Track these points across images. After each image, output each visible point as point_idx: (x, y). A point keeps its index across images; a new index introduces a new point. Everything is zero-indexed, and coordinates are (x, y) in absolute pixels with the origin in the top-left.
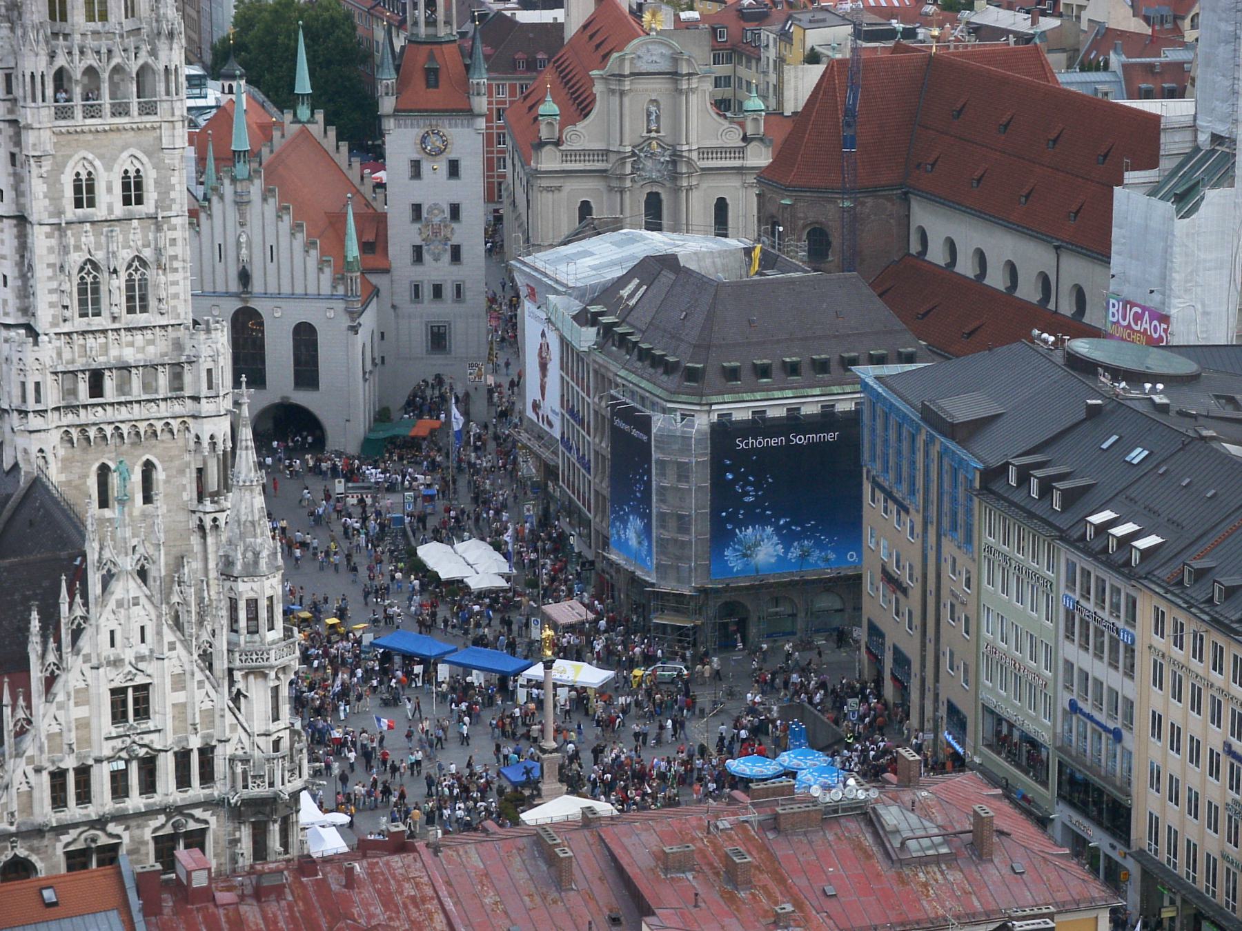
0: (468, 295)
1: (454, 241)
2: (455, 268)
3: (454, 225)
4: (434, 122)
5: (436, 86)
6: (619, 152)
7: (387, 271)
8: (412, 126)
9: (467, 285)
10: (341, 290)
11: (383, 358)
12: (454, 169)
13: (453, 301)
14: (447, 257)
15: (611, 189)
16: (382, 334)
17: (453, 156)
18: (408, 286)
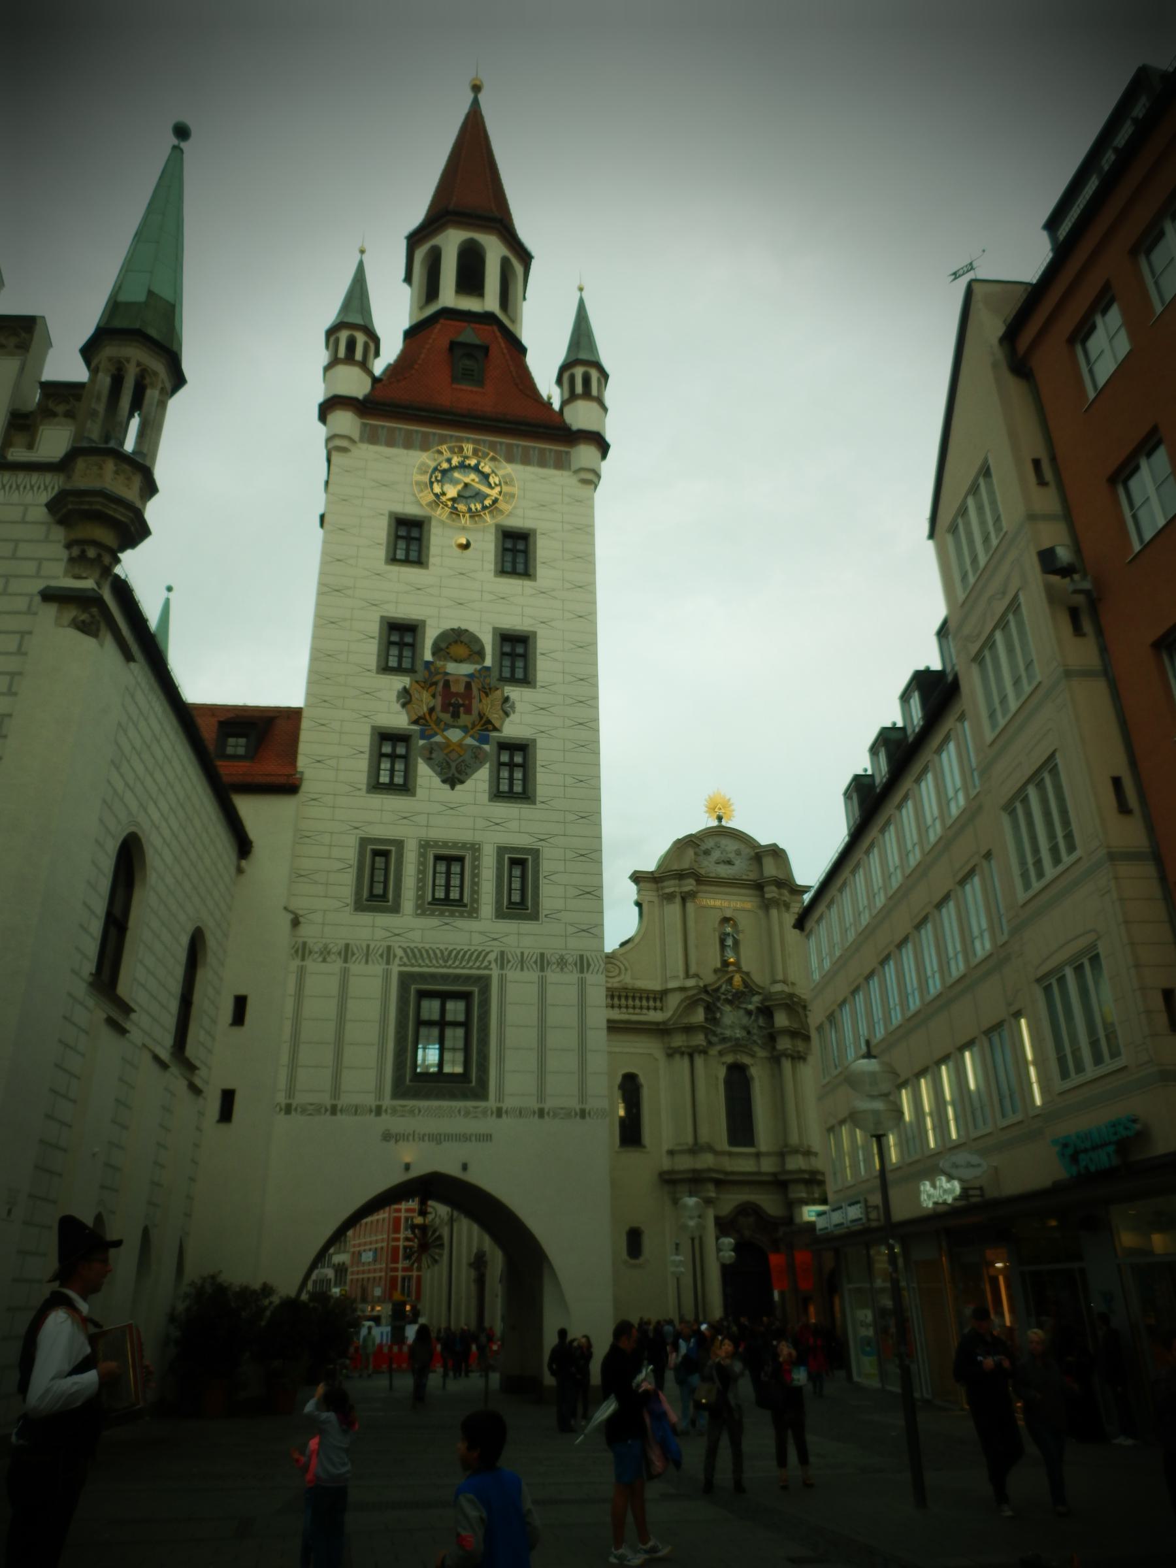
0: (550, 895)
1: (512, 729)
2: (505, 810)
3: (514, 693)
4: (468, 448)
5: (480, 382)
6: (682, 989)
7: (289, 787)
8: (408, 445)
9: (546, 866)
10: (54, 441)
11: (228, 1097)
12: (516, 552)
13: (500, 914)
14: (481, 778)
15: (671, 1053)
16: (241, 1003)
17: (517, 521)
18: (351, 855)
